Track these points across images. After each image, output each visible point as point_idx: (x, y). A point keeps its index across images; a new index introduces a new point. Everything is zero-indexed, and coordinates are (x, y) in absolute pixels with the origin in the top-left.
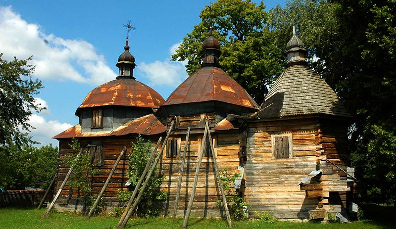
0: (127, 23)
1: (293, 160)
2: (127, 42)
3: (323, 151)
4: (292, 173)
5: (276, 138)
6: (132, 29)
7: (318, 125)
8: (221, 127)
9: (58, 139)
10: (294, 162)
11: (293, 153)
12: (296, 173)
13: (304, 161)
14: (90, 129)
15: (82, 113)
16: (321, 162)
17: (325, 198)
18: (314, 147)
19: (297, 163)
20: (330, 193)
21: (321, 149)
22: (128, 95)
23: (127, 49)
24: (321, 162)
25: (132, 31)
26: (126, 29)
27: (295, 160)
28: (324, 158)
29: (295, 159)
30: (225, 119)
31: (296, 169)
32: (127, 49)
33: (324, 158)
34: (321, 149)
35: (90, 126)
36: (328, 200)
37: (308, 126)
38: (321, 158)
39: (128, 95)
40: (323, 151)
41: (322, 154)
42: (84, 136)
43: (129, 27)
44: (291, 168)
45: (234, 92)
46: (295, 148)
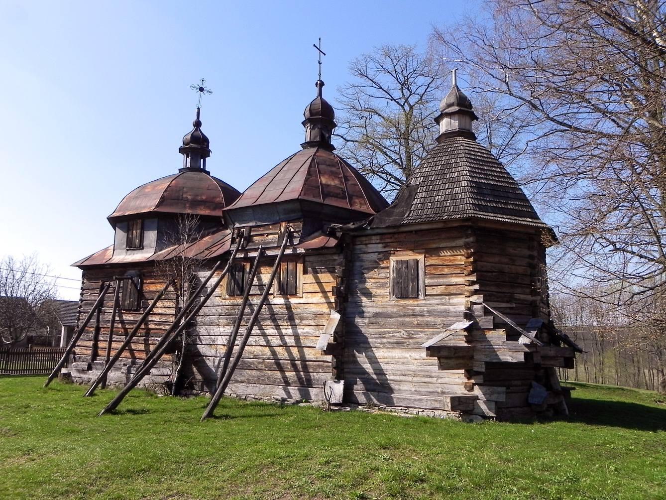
1: (424, 302)
3: (477, 287)
5: (397, 262)
7: (471, 239)
9: (80, 267)
10: (426, 305)
12: (428, 325)
13: (443, 304)
19: (431, 308)
20: (487, 363)
21: (473, 283)
23: (198, 124)
25: (205, 96)
27: (428, 302)
29: (428, 300)
31: (429, 319)
32: (198, 124)
34: (473, 283)
35: (125, 246)
36: (482, 376)
37: (454, 241)
38: (474, 299)
40: (477, 287)
41: (476, 292)
46: (428, 281)
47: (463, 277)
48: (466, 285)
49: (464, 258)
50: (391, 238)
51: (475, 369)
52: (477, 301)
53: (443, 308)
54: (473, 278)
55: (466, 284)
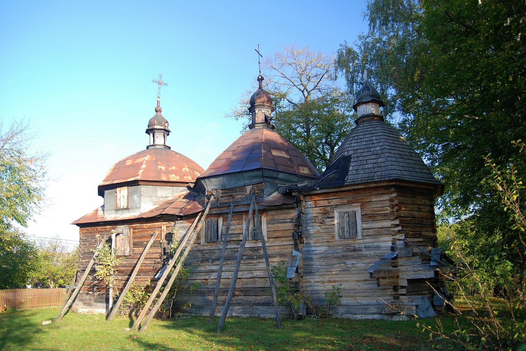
0: (157, 78)
1: (362, 241)
2: (158, 102)
3: (400, 228)
4: (359, 257)
6: (164, 86)
7: (394, 195)
8: (271, 201)
11: (363, 232)
14: (114, 212)
15: (102, 190)
16: (398, 242)
17: (403, 287)
18: (387, 224)
19: (367, 245)
20: (409, 281)
21: (397, 226)
22: (159, 167)
24: (398, 242)
25: (163, 88)
26: (156, 86)
27: (365, 241)
28: (402, 236)
29: (365, 239)
30: (277, 192)
31: (366, 253)
33: (402, 236)
34: (397, 226)
38: (397, 237)
39: (159, 167)
40: (400, 228)
41: (399, 231)
42: (107, 220)
43: (160, 83)
44: (360, 250)
45: (288, 157)
46: (365, 226)
47: (390, 221)
48: (392, 228)
49: (389, 208)
50: (334, 196)
51: (400, 284)
52: (400, 238)
53: (375, 244)
54: (397, 222)
55: (392, 227)
